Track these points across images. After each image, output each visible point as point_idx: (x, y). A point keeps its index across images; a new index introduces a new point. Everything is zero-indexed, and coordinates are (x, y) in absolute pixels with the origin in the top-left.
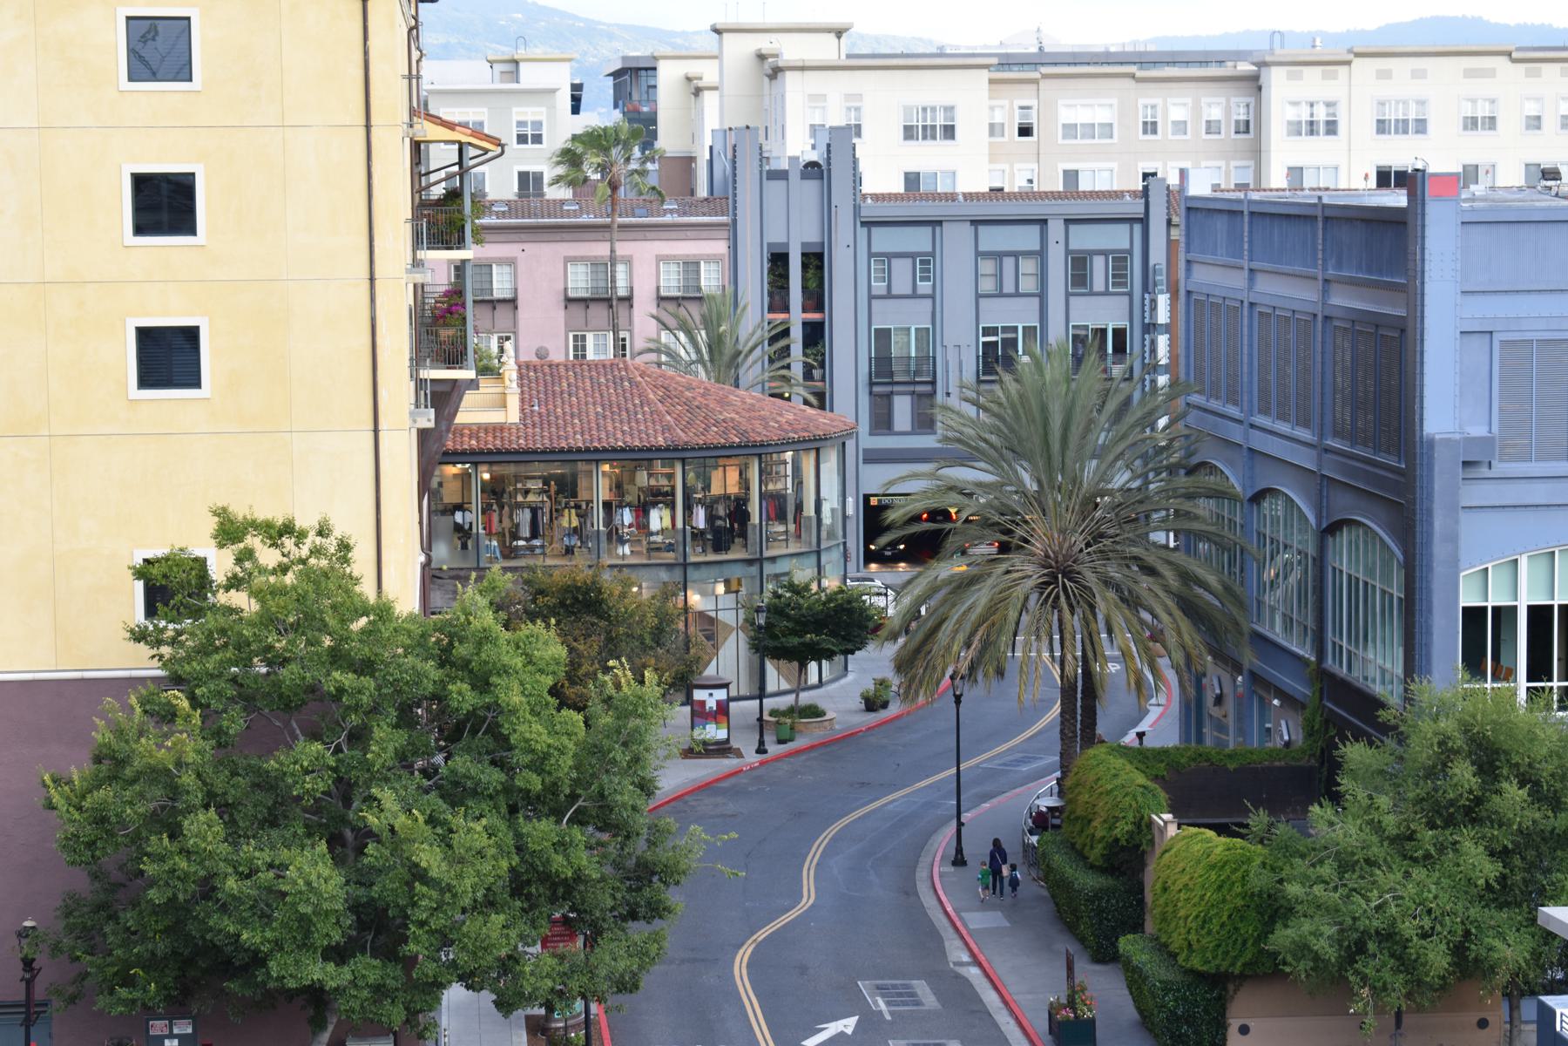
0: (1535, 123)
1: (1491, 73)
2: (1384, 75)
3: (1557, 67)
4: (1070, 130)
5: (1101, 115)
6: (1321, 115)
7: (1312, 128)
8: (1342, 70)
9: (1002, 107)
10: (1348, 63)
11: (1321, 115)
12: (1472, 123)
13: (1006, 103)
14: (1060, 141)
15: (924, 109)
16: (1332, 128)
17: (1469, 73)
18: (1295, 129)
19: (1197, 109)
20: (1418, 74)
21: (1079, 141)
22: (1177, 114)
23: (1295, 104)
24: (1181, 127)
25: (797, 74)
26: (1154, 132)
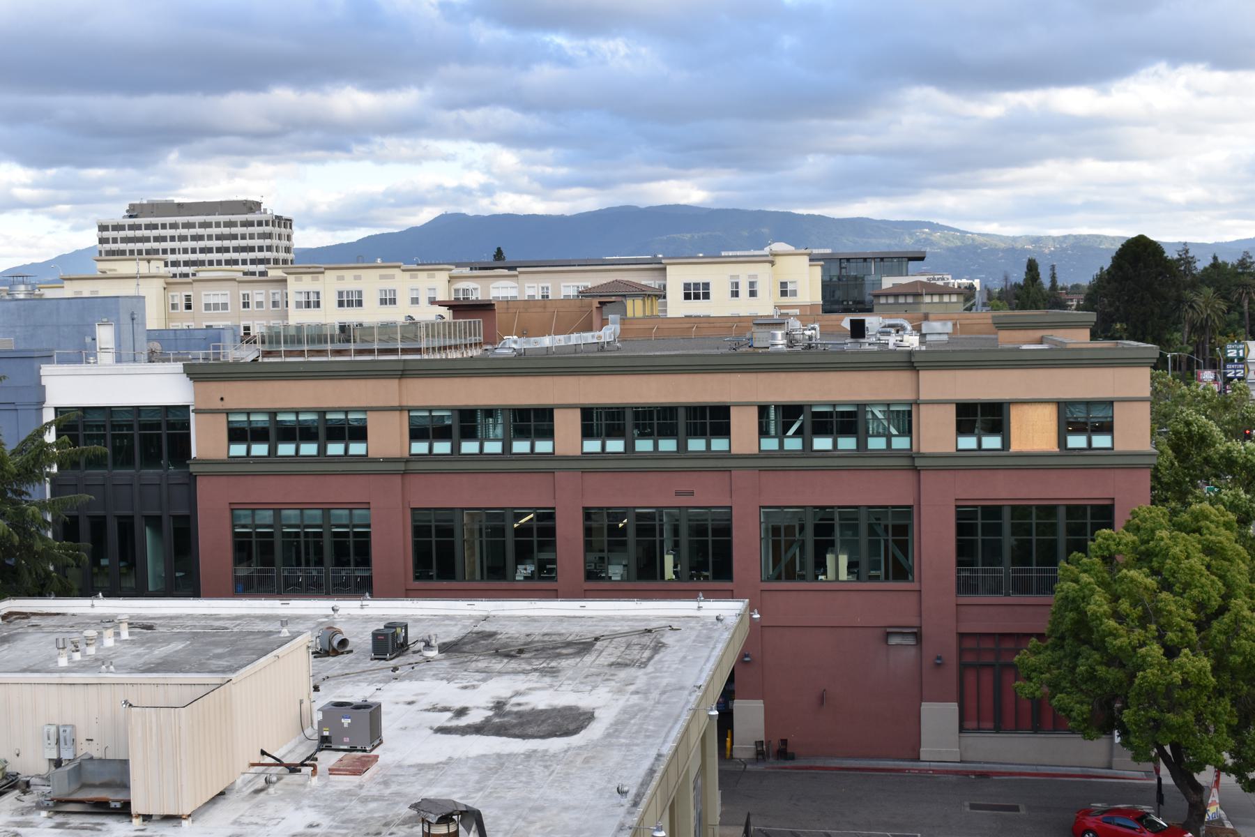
0: (415, 301)
1: (393, 277)
2: (341, 278)
3: (425, 273)
4: (208, 306)
5: (220, 300)
6: (313, 298)
7: (308, 305)
8: (321, 276)
9: (173, 297)
10: (323, 273)
11: (313, 298)
12: (383, 302)
13: (178, 294)
14: (204, 311)
15: (386, 291)
16: (318, 305)
17: (382, 277)
18: (299, 305)
19: (267, 296)
20: (357, 278)
21: (212, 311)
22: (259, 299)
23: (301, 293)
24: (260, 304)
25: (69, 282)
26: (244, 307)
